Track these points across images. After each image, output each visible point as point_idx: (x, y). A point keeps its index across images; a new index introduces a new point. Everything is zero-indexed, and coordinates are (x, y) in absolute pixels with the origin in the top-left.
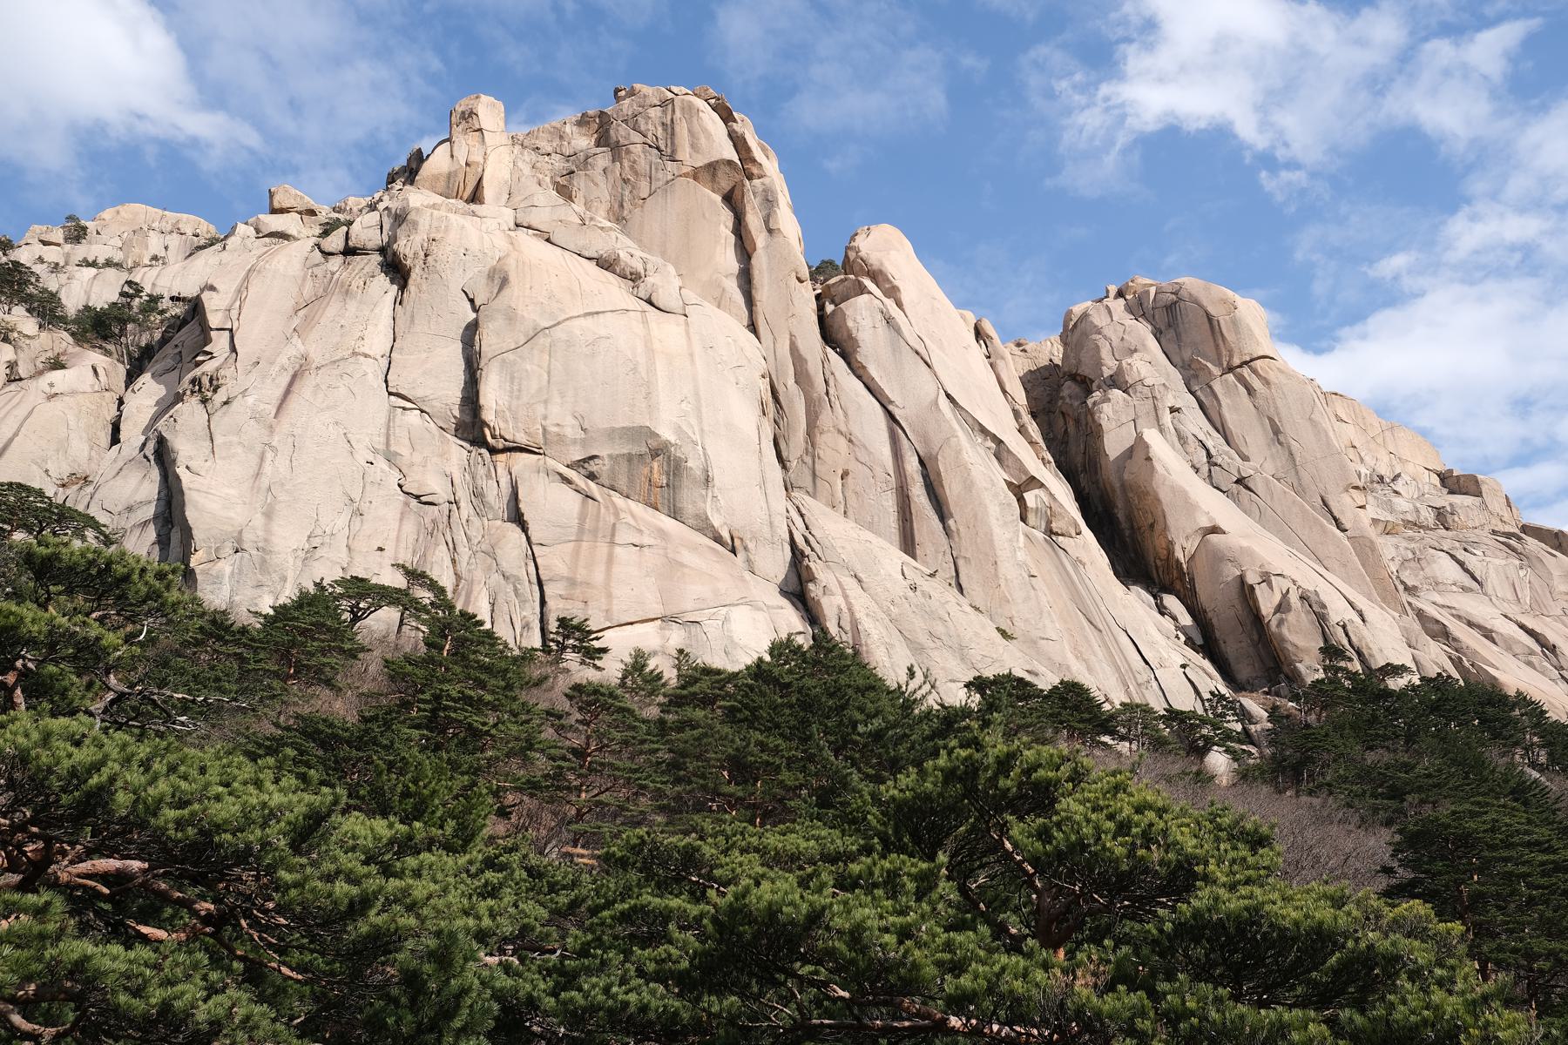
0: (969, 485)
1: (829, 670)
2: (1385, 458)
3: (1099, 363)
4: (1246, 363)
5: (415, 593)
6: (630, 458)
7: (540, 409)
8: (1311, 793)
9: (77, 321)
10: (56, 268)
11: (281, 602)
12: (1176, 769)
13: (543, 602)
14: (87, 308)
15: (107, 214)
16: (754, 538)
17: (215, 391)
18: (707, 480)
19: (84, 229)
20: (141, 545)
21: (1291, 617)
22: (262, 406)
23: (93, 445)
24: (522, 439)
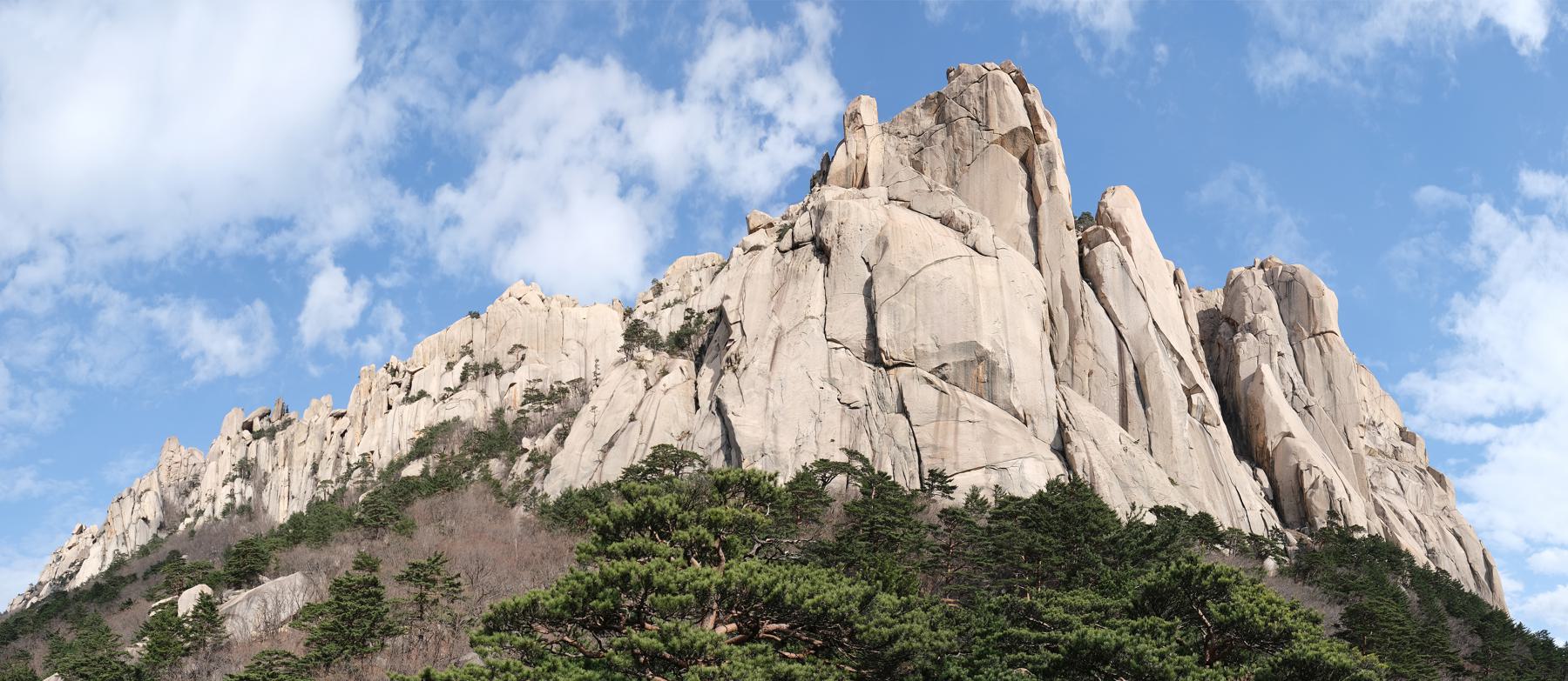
0: (1161, 386)
1: (1078, 498)
6: (965, 363)
9: (668, 343)
13: (920, 461)
21: (1317, 492)
24: (903, 357)
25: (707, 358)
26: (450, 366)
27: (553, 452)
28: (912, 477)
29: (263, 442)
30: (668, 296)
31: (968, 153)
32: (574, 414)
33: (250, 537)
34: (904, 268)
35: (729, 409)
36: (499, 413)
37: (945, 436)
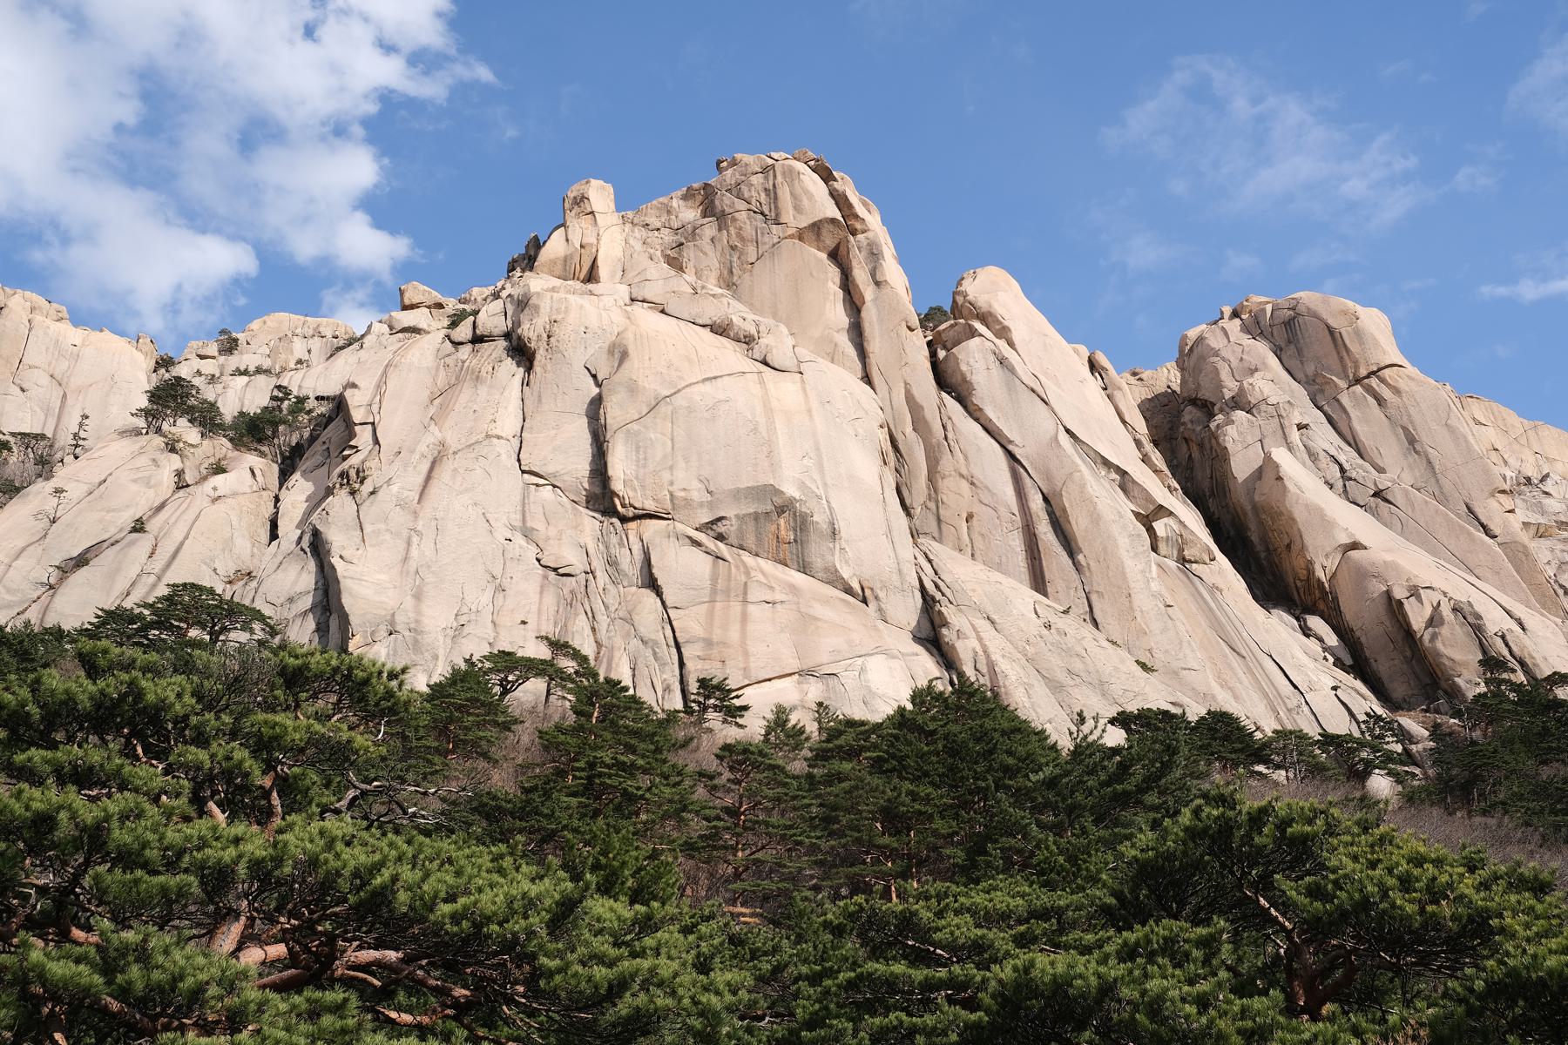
0: (1096, 519)
1: (972, 715)
2: (1531, 459)
3: (1219, 386)
4: (1374, 373)
5: (560, 664)
7: (666, 476)
8: (1484, 813)
9: (235, 426)
10: (212, 379)
11: (436, 679)
13: (682, 664)
14: (242, 414)
15: (255, 325)
16: (884, 587)
17: (362, 482)
19: (236, 340)
21: (1445, 631)
22: (406, 493)
23: (255, 542)
24: (651, 506)
25: (306, 464)
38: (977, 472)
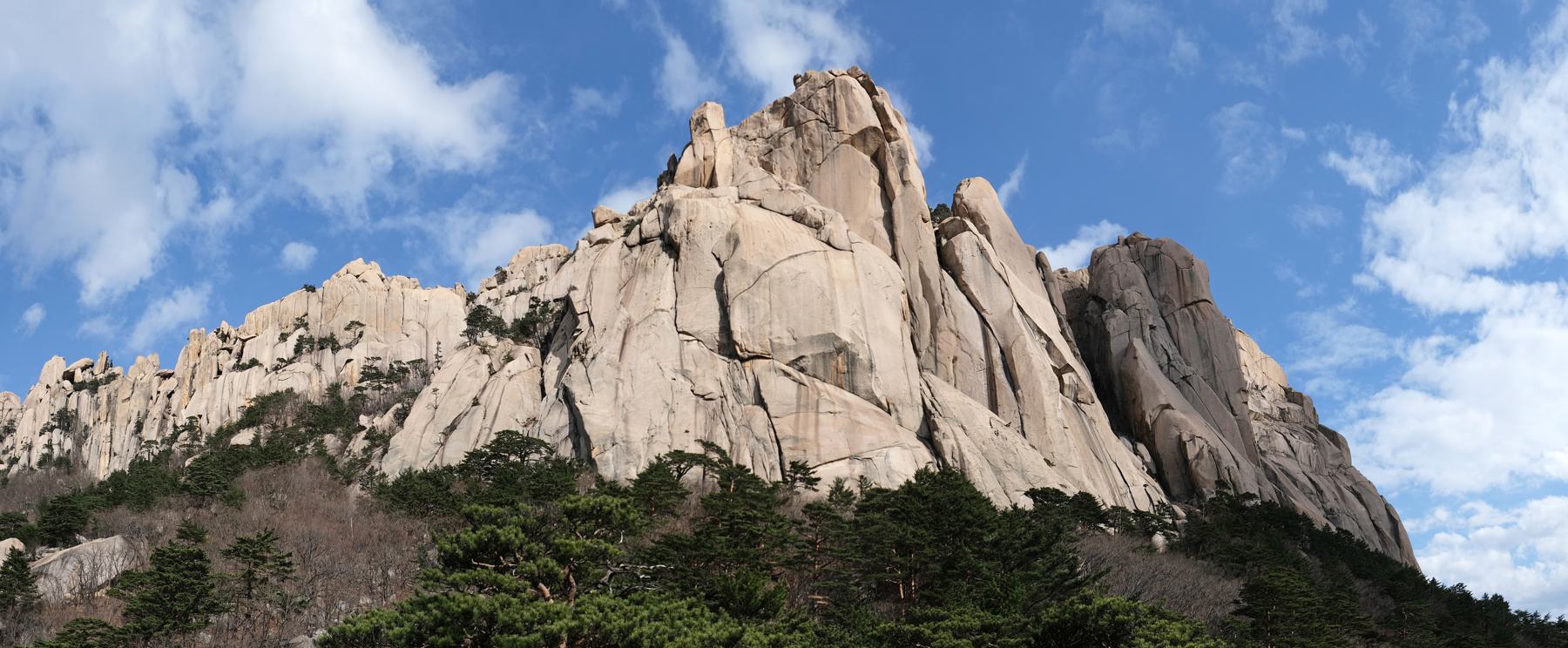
0: (1030, 368)
3: (1110, 290)
6: (824, 355)
7: (768, 329)
9: (513, 329)
11: (641, 470)
12: (1137, 544)
16: (901, 403)
18: (872, 367)
20: (566, 451)
23: (534, 400)
24: (758, 350)
25: (554, 346)
26: (284, 337)
27: (392, 432)
28: (773, 468)
29: (84, 394)
30: (512, 284)
31: (818, 152)
32: (414, 395)
33: (68, 492)
34: (756, 264)
35: (577, 398)
36: (334, 389)
37: (805, 428)
38: (962, 330)
